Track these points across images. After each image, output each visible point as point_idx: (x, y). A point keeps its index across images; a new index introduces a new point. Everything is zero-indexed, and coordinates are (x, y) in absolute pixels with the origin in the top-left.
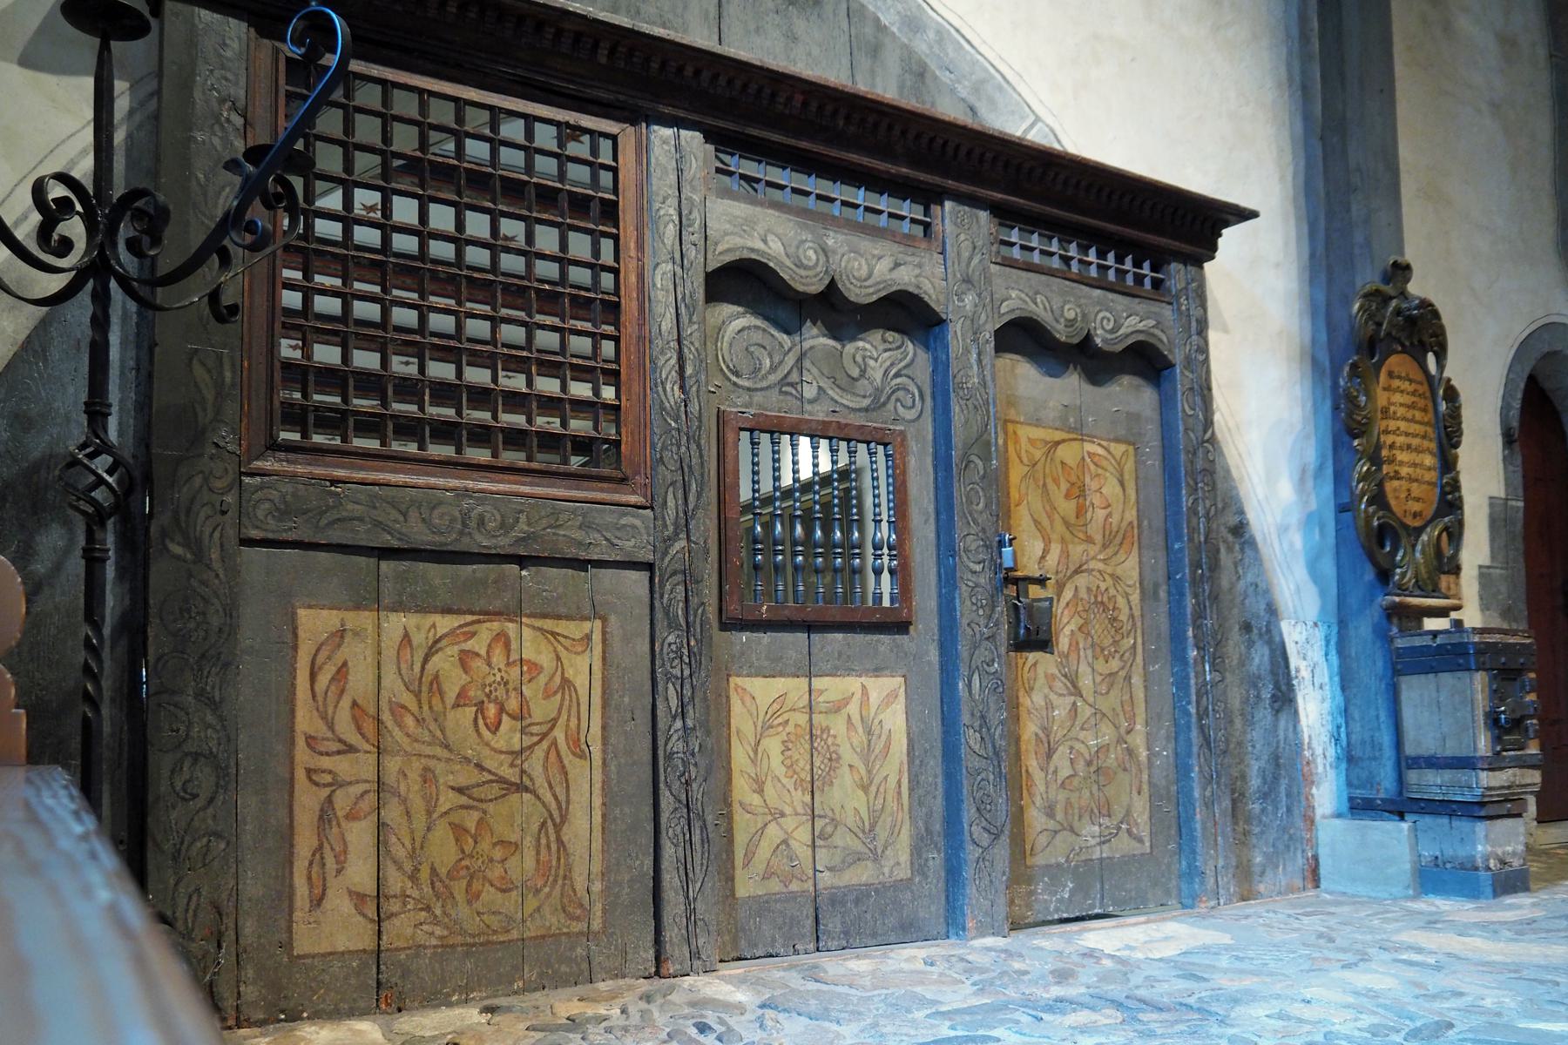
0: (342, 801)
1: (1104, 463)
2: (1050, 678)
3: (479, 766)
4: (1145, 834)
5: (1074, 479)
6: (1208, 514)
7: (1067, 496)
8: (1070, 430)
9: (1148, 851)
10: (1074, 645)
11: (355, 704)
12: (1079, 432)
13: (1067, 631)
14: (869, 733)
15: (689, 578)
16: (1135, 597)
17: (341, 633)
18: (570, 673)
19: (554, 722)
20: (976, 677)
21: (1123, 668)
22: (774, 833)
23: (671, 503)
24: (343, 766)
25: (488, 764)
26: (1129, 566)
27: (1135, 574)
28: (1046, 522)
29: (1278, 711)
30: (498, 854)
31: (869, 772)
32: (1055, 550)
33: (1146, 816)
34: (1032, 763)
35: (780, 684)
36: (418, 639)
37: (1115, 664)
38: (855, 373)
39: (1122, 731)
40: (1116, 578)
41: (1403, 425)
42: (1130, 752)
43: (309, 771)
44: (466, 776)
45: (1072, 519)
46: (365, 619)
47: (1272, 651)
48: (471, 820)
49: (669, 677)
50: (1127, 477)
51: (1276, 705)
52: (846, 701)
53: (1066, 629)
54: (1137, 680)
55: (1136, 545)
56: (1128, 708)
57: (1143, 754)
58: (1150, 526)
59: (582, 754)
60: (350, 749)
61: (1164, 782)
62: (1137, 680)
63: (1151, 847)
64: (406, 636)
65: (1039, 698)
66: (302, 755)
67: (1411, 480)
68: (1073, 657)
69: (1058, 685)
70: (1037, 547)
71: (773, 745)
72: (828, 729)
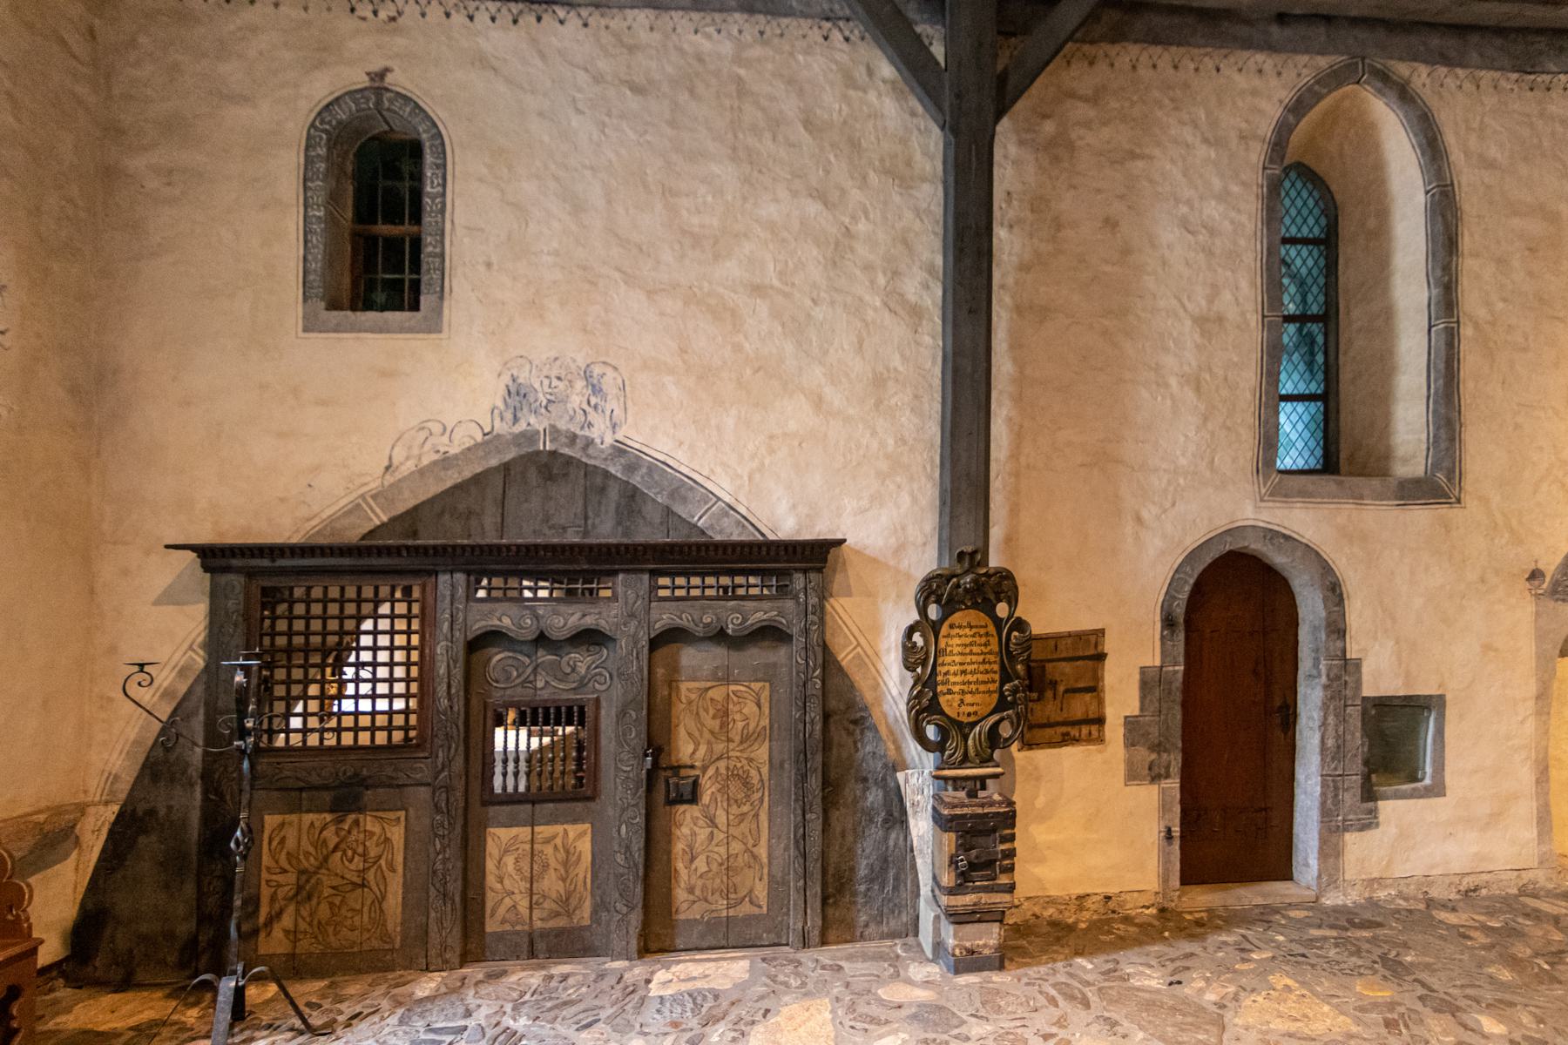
0: (281, 893)
1: (746, 695)
2: (695, 821)
3: (343, 878)
5: (719, 707)
7: (714, 717)
8: (719, 679)
10: (714, 799)
11: (288, 853)
12: (727, 679)
13: (709, 792)
14: (567, 852)
15: (448, 789)
16: (765, 770)
17: (282, 825)
18: (389, 835)
19: (380, 857)
20: (624, 827)
22: (508, 902)
23: (441, 754)
24: (280, 878)
25: (348, 876)
26: (762, 752)
27: (766, 757)
28: (697, 734)
30: (350, 915)
31: (567, 871)
32: (703, 749)
34: (680, 866)
35: (514, 831)
36: (317, 824)
37: (745, 809)
38: (568, 670)
39: (750, 846)
40: (750, 760)
41: (958, 659)
43: (267, 881)
44: (336, 882)
45: (717, 729)
46: (294, 817)
47: (886, 794)
48: (337, 901)
49: (436, 835)
50: (762, 701)
52: (554, 837)
53: (708, 791)
58: (779, 727)
59: (394, 871)
60: (285, 871)
62: (764, 817)
64: (312, 824)
65: (685, 830)
66: (265, 875)
67: (963, 692)
68: (713, 805)
69: (701, 823)
70: (691, 748)
71: (509, 860)
72: (542, 852)
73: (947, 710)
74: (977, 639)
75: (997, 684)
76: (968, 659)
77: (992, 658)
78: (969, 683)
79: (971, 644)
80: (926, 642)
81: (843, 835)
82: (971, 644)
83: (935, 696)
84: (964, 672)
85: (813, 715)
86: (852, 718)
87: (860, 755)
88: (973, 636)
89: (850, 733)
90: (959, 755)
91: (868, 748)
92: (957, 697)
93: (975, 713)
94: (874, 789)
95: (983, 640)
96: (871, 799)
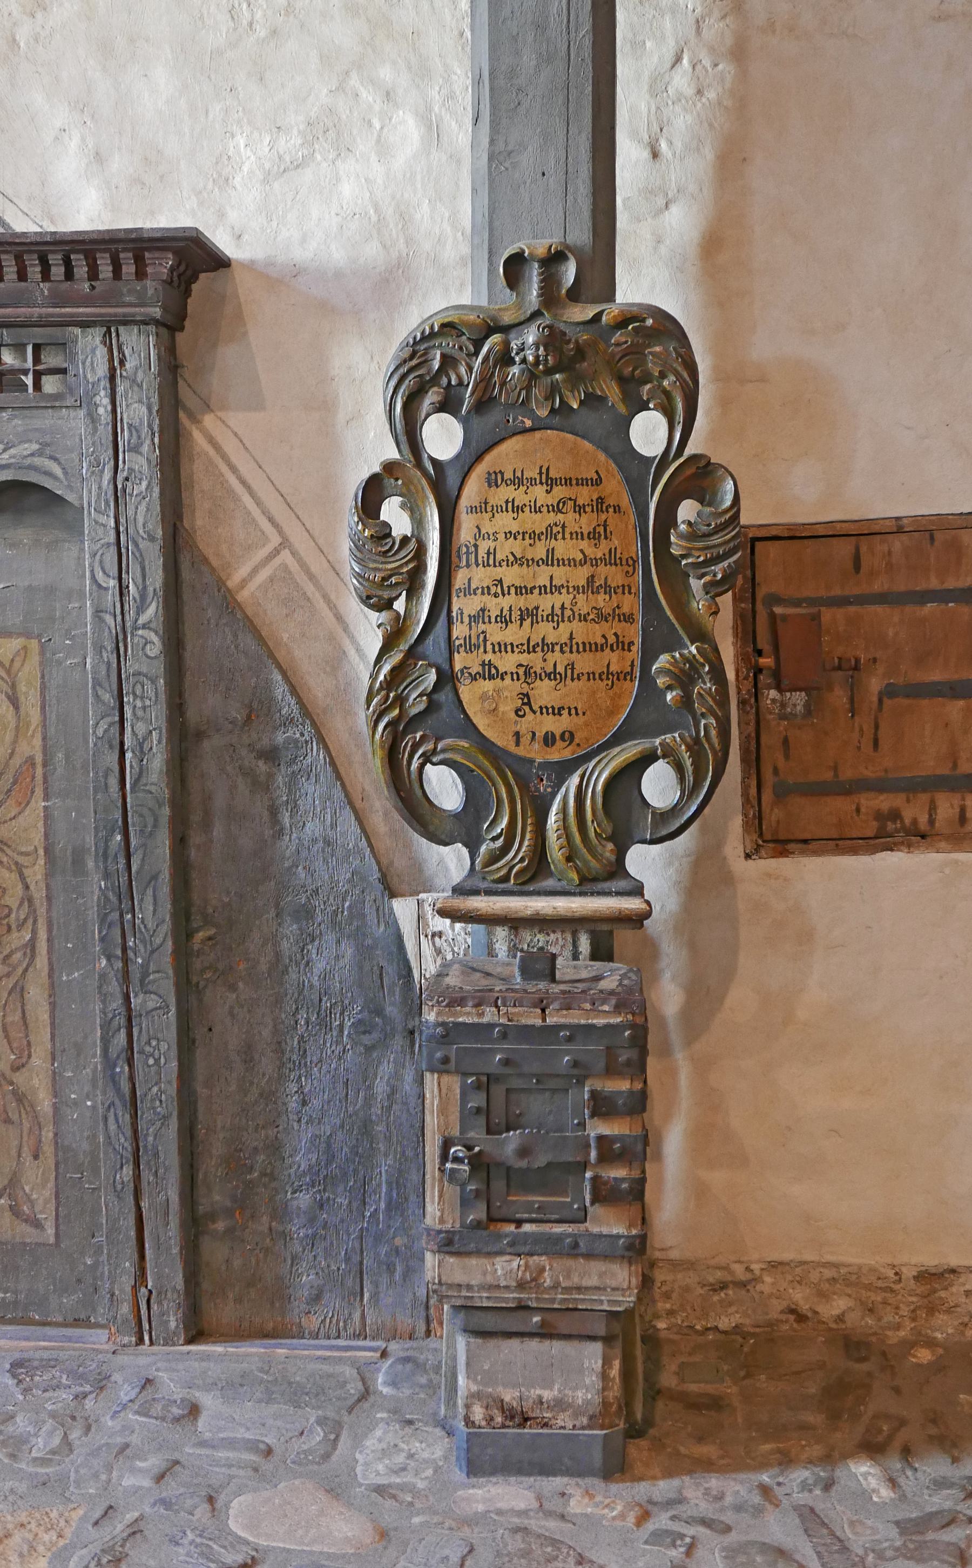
4: (47, 1216)
6: (141, 745)
9: (52, 1240)
16: (36, 872)
21: (8, 975)
27: (37, 837)
29: (369, 1049)
33: (49, 1191)
41: (511, 576)
42: (20, 1098)
47: (364, 952)
50: (22, 688)
51: (367, 1040)
54: (36, 994)
55: (39, 792)
56: (16, 1034)
57: (45, 1104)
61: (85, 1146)
62: (36, 994)
63: (57, 1235)
73: (481, 722)
74: (569, 518)
75: (636, 652)
76: (543, 576)
77: (615, 576)
78: (547, 647)
79: (549, 533)
80: (419, 522)
81: (248, 1053)
82: (549, 533)
83: (447, 678)
84: (529, 615)
85: (141, 728)
86: (265, 742)
87: (288, 845)
88: (557, 509)
89: (262, 786)
90: (523, 847)
91: (313, 828)
92: (511, 688)
93: (569, 737)
94: (330, 937)
95: (586, 523)
96: (320, 965)
